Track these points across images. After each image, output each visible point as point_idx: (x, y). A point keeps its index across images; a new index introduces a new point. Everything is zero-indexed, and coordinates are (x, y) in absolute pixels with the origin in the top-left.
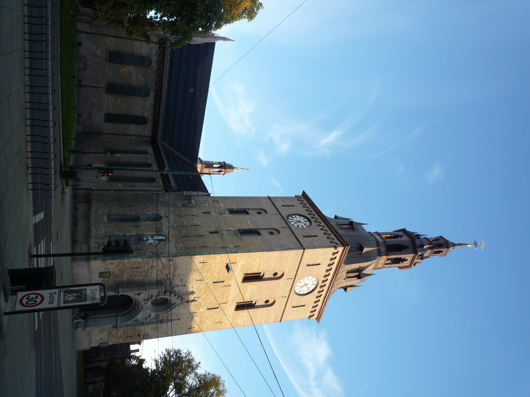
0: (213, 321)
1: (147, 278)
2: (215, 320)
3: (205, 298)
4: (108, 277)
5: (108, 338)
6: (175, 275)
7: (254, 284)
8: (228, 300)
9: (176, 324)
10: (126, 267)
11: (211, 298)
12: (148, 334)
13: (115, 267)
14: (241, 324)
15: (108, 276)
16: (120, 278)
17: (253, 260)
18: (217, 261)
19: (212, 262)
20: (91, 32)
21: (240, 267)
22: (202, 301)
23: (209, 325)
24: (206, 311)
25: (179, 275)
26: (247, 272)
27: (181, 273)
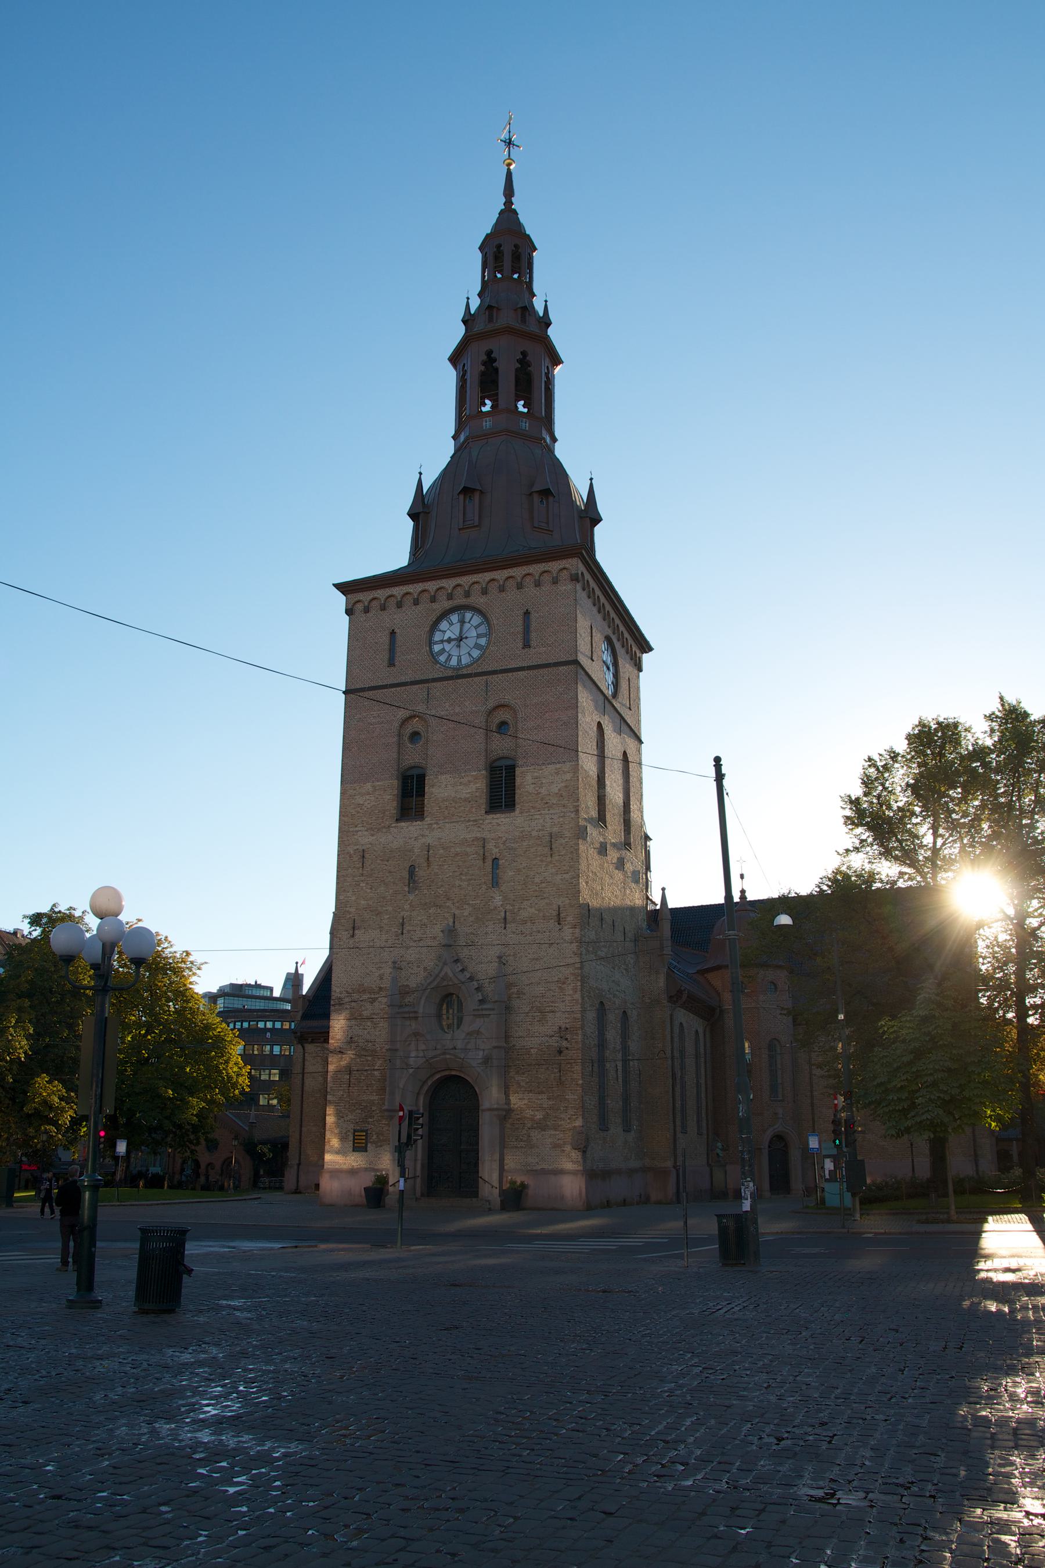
0: (542, 861)
1: (379, 1049)
2: (539, 858)
3: (458, 902)
4: (367, 1134)
5: (556, 1130)
6: (381, 988)
7: (433, 786)
8: (473, 841)
9: (537, 959)
10: (345, 1096)
11: (460, 886)
12: (560, 1028)
13: (342, 1119)
14: (568, 776)
15: (364, 1134)
16: (374, 1108)
17: (361, 811)
18: (354, 898)
19: (353, 910)
20: (296, 1167)
21: (374, 838)
22: (467, 907)
23: (554, 870)
24: (502, 888)
25: (381, 979)
26: (390, 817)
27: (377, 974)
